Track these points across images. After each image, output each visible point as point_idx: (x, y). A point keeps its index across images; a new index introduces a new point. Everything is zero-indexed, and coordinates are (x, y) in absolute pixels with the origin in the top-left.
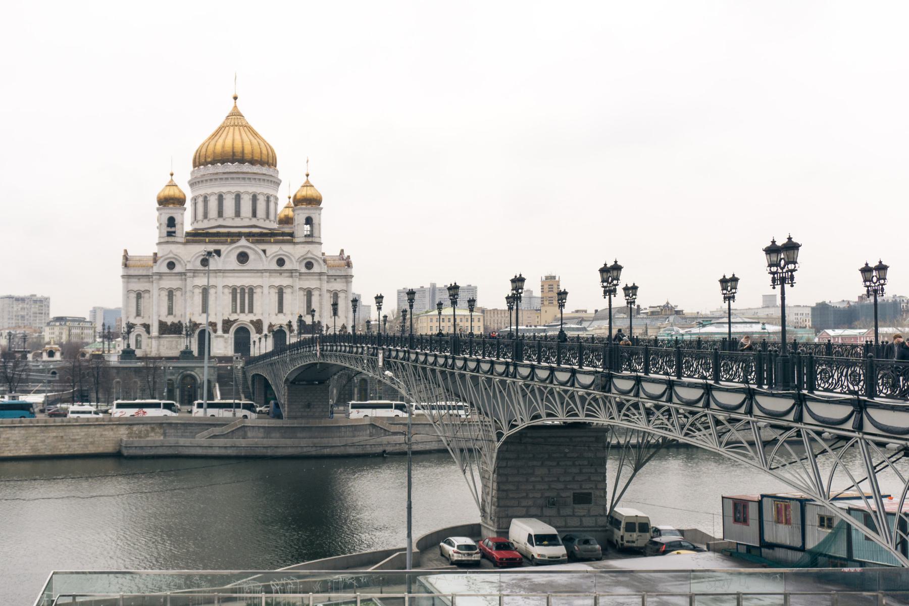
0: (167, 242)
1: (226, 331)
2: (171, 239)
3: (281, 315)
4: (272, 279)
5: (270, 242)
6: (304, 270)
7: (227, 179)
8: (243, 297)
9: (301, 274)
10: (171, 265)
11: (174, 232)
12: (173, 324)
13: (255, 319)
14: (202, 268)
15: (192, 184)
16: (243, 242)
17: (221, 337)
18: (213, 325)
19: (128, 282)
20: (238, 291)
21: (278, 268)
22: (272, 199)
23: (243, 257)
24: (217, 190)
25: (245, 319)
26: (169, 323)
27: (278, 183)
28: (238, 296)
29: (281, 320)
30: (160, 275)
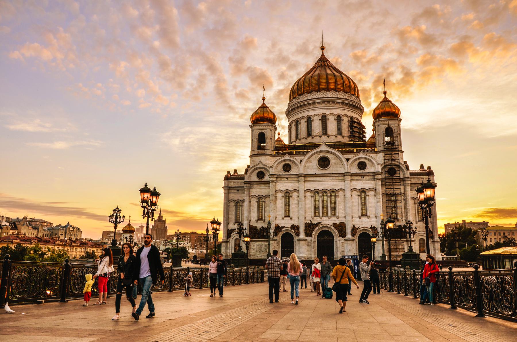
3: (364, 219)
4: (354, 183)
5: (352, 152)
7: (314, 103)
8: (325, 199)
10: (261, 175)
12: (263, 228)
13: (337, 222)
15: (289, 113)
16: (323, 148)
17: (303, 240)
18: (295, 228)
19: (228, 193)
21: (359, 171)
23: (324, 162)
24: (306, 114)
26: (259, 228)
27: (361, 110)
29: (365, 224)
30: (251, 184)
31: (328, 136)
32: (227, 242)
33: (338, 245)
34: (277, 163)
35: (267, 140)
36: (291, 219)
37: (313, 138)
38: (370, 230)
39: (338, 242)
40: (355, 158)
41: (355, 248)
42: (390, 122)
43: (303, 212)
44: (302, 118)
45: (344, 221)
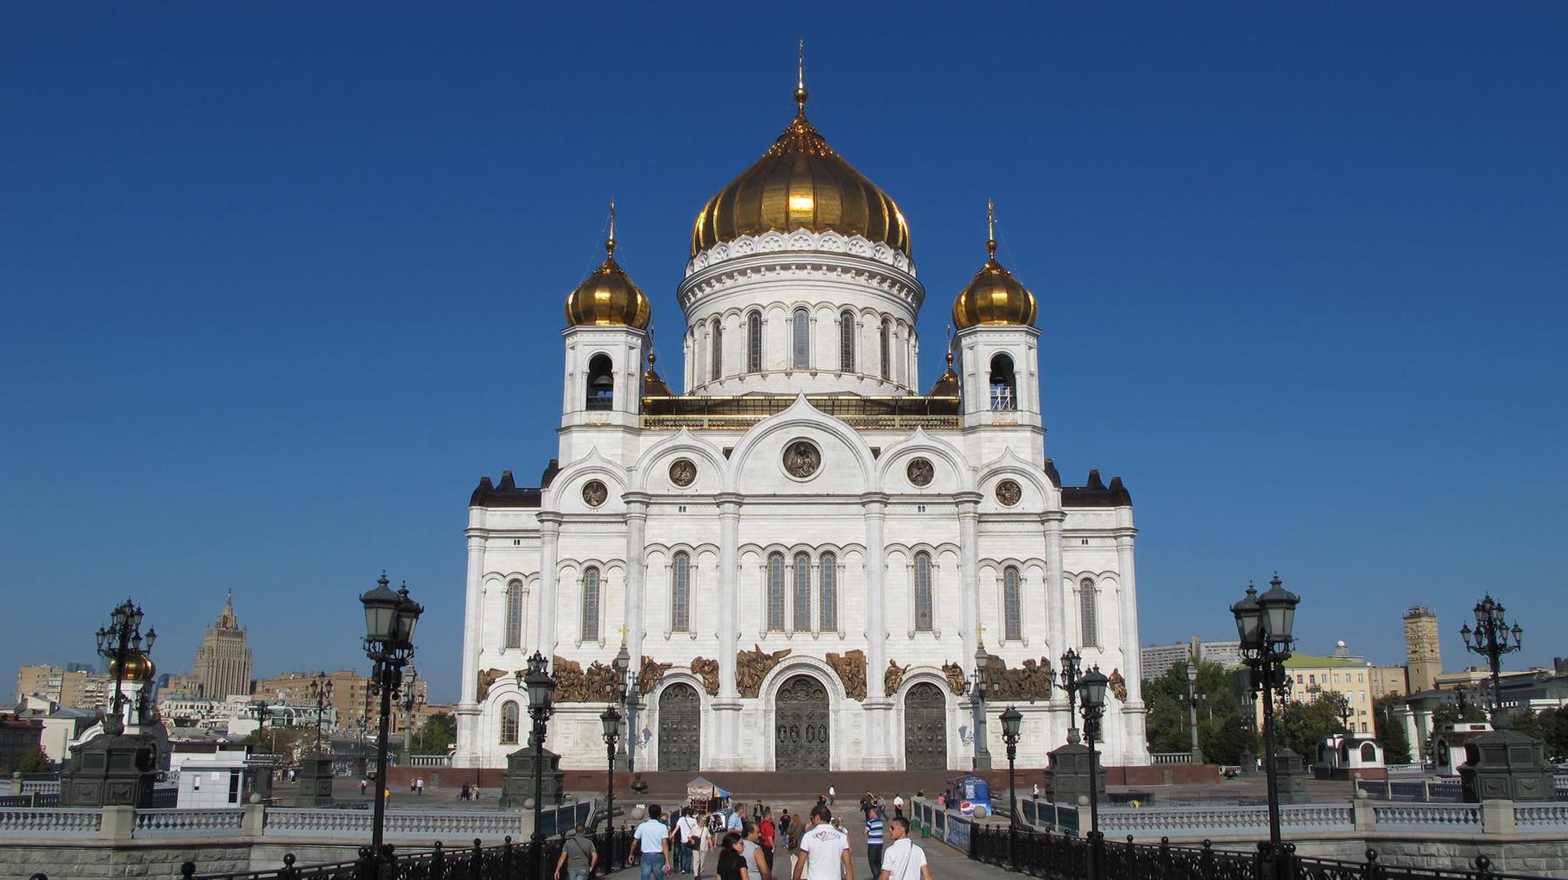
1: (748, 686)
2: (597, 416)
3: (924, 638)
4: (891, 525)
6: (991, 504)
9: (981, 519)
10: (594, 492)
11: (610, 400)
12: (597, 669)
13: (841, 650)
14: (676, 490)
16: (801, 410)
18: (707, 668)
20: (789, 560)
21: (910, 488)
22: (893, 327)
25: (811, 649)
26: (584, 668)
28: (789, 576)
31: (814, 374)
32: (475, 713)
33: (843, 725)
34: (651, 456)
35: (618, 382)
36: (694, 638)
38: (944, 675)
39: (843, 713)
40: (900, 447)
41: (893, 731)
43: (729, 619)
45: (863, 646)
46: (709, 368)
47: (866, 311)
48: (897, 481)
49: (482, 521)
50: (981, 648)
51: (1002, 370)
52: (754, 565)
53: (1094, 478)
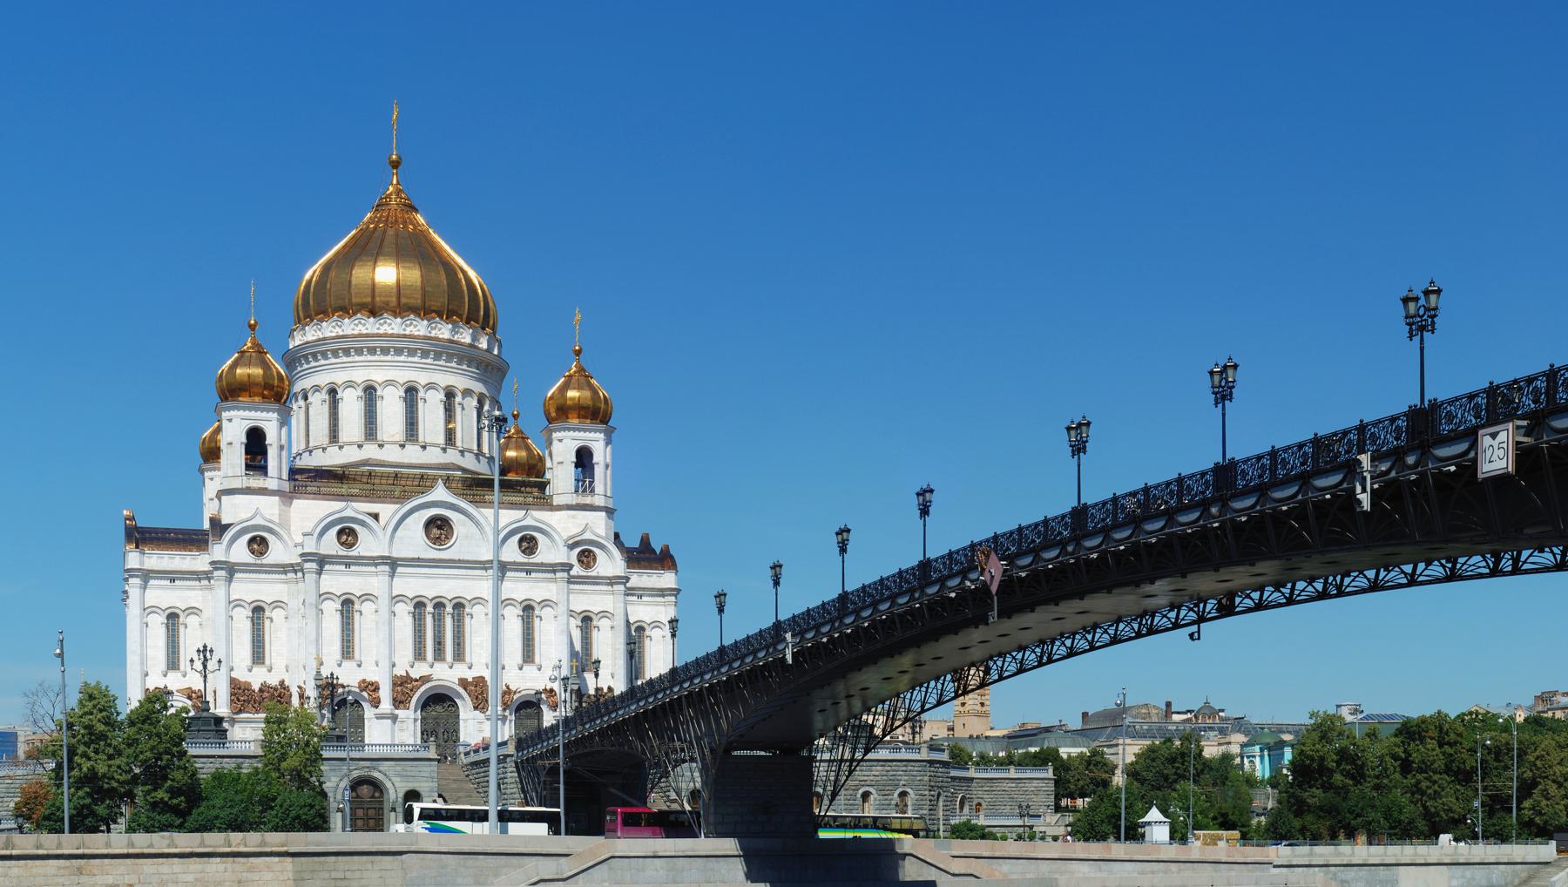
0: (248, 491)
2: (256, 482)
10: (258, 544)
13: (470, 675)
14: (342, 552)
16: (440, 493)
25: (447, 674)
28: (429, 620)
31: (424, 447)
37: (381, 446)
42: (588, 435)
43: (383, 652)
44: (350, 384)
46: (326, 431)
47: (467, 392)
48: (511, 552)
49: (142, 563)
50: (597, 675)
51: (584, 458)
52: (404, 611)
53: (645, 541)
